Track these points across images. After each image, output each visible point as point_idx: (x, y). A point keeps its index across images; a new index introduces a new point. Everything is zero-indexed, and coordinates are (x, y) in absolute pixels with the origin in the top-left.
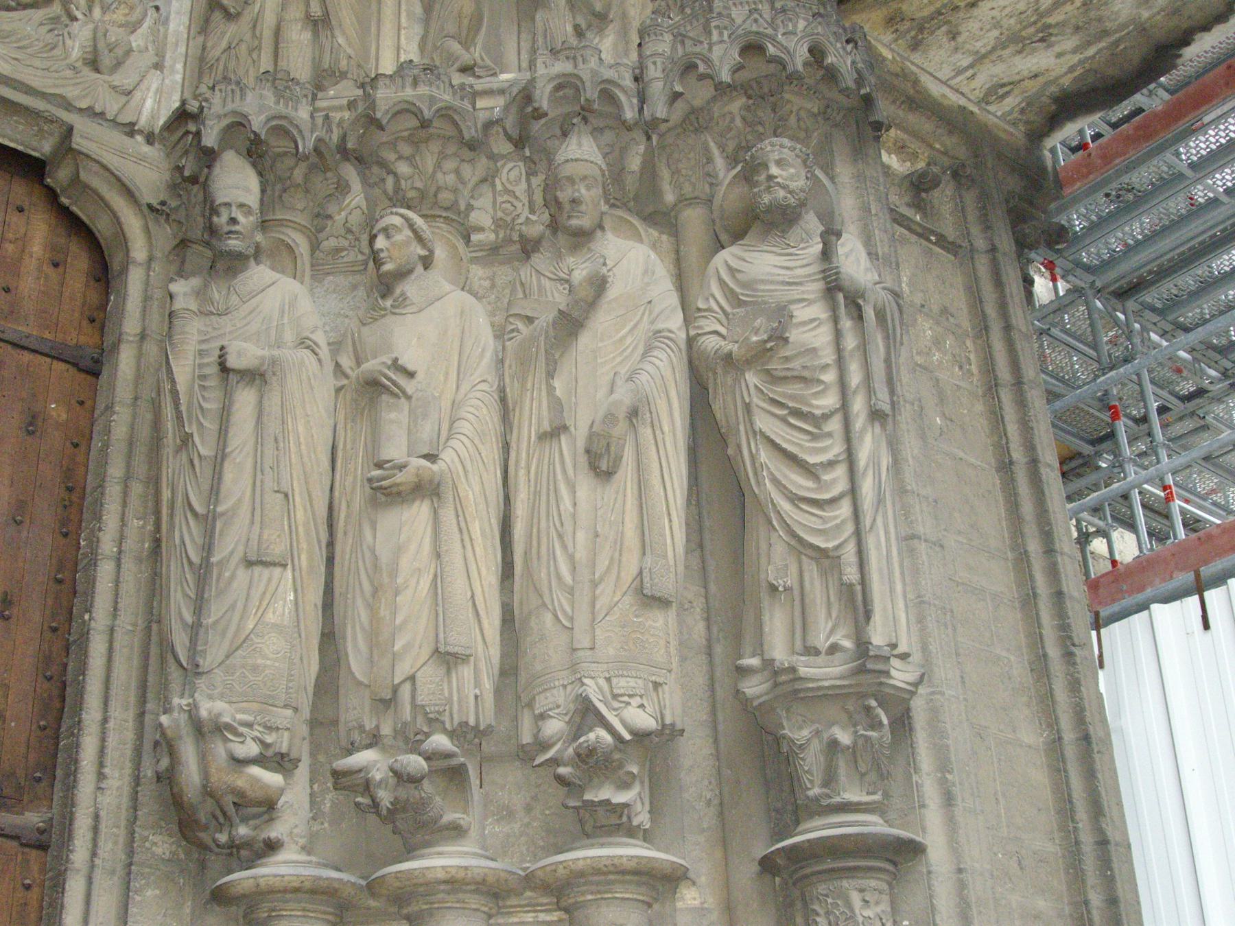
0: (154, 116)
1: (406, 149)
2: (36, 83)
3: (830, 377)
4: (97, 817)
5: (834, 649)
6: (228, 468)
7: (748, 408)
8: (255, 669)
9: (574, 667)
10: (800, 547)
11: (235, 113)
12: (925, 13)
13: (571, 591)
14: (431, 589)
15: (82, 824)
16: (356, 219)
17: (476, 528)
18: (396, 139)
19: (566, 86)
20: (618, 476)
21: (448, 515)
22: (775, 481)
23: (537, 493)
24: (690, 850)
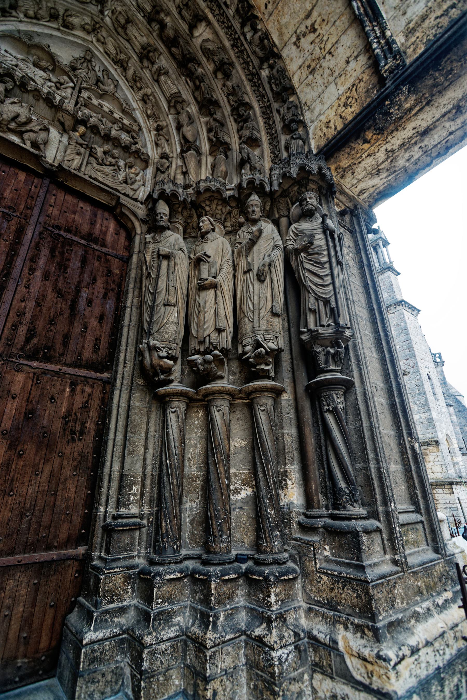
1: (208, 203)
2: (110, 184)
3: (325, 253)
4: (123, 374)
5: (329, 325)
6: (160, 280)
7: (302, 262)
8: (166, 333)
9: (254, 332)
10: (318, 298)
14: (214, 312)
15: (119, 375)
16: (195, 225)
17: (227, 296)
19: (251, 182)
22: (311, 281)
23: (243, 287)
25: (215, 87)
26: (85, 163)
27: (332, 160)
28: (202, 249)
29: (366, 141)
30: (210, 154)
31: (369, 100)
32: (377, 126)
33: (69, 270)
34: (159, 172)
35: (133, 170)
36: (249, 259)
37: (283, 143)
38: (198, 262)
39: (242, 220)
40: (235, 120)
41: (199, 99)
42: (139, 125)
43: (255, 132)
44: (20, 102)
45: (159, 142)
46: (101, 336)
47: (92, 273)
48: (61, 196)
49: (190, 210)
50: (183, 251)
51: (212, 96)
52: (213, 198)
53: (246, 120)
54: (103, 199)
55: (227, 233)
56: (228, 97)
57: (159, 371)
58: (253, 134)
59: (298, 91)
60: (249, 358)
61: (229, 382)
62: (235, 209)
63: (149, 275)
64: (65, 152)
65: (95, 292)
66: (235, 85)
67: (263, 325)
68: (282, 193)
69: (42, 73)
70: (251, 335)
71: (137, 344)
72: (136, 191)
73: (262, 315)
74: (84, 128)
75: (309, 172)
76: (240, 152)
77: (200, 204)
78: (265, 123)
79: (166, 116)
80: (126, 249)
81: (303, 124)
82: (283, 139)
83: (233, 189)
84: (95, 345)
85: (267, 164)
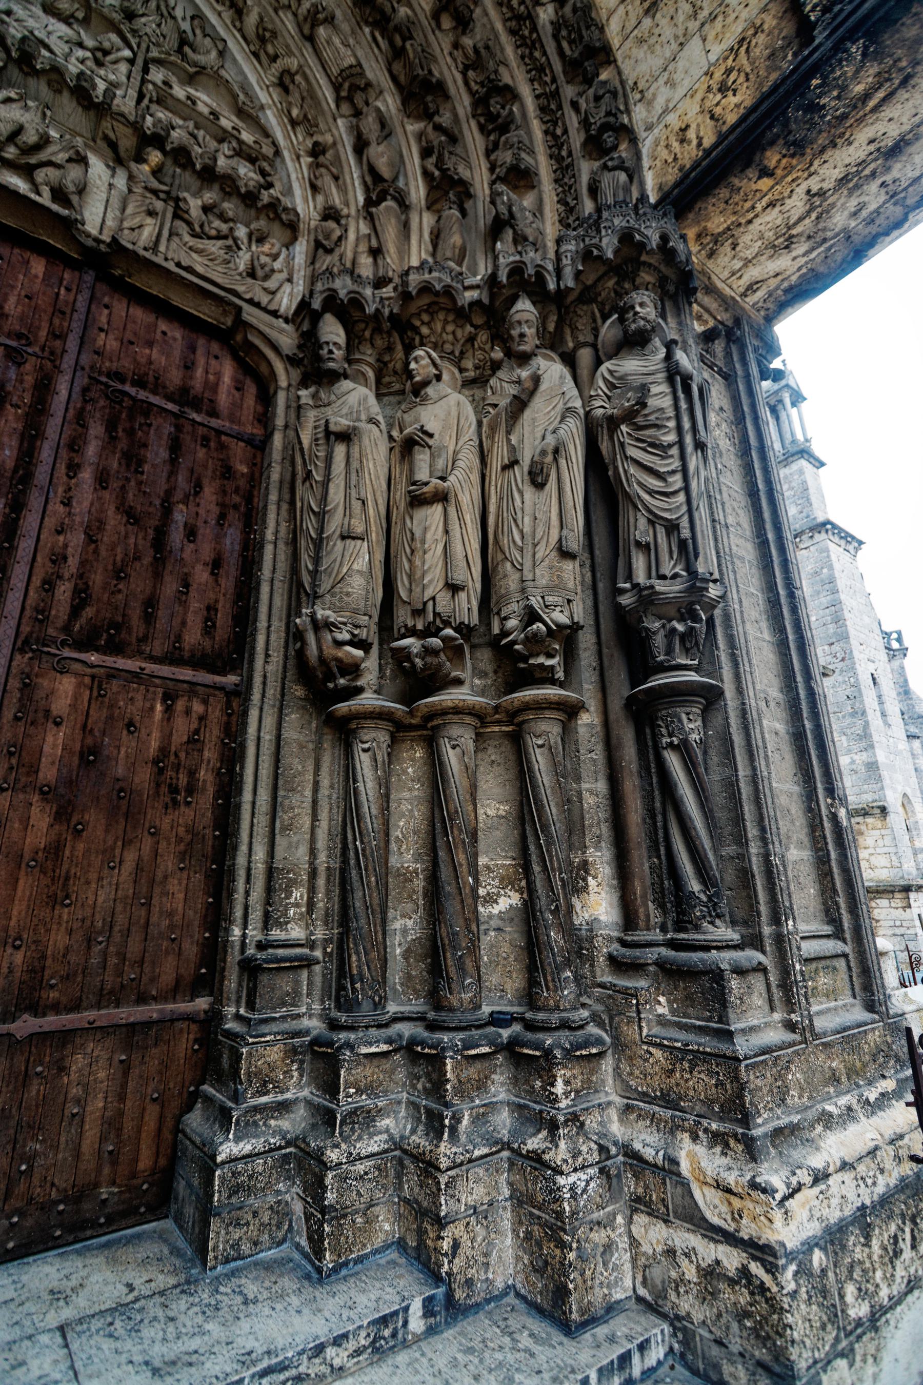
0: (288, 308)
1: (425, 317)
2: (219, 280)
3: (672, 424)
4: (265, 677)
5: (675, 576)
6: (332, 486)
7: (622, 445)
8: (348, 594)
9: (523, 590)
11: (329, 289)
12: (721, 229)
13: (521, 550)
14: (444, 548)
15: (257, 680)
16: (399, 366)
19: (517, 270)
20: (548, 487)
21: (452, 511)
22: (640, 484)
23: (501, 498)
24: (587, 691)
25: (438, 50)
26: (166, 233)
27: (691, 216)
28: (417, 420)
29: (766, 173)
30: (428, 208)
31: (774, 76)
32: (791, 138)
33: (146, 468)
34: (320, 251)
35: (266, 248)
36: (514, 439)
37: (585, 179)
38: (408, 447)
39: (498, 354)
40: (482, 128)
41: (402, 78)
42: (274, 144)
43: (523, 155)
44: (22, 98)
45: (319, 183)
46: (217, 601)
47: (192, 471)
48: (120, 307)
49: (388, 333)
50: (377, 423)
51: (430, 72)
52: (436, 308)
53: (504, 129)
54: (205, 312)
55: (468, 384)
56: (464, 74)
57: (335, 670)
58: (519, 159)
59: (619, 56)
60: (514, 642)
61: (475, 692)
62: (484, 330)
63: (308, 475)
64: (123, 210)
65: (202, 512)
66: (480, 45)
67: (543, 576)
68: (582, 293)
69: (62, 29)
70: (517, 596)
71: (289, 616)
72: (274, 293)
73: (539, 556)
74: (159, 154)
75: (642, 246)
76: (493, 202)
77: (409, 322)
78: (546, 132)
79: (330, 120)
80: (259, 421)
81: (628, 133)
82: (586, 169)
83: (477, 287)
84: (207, 619)
85: (551, 229)
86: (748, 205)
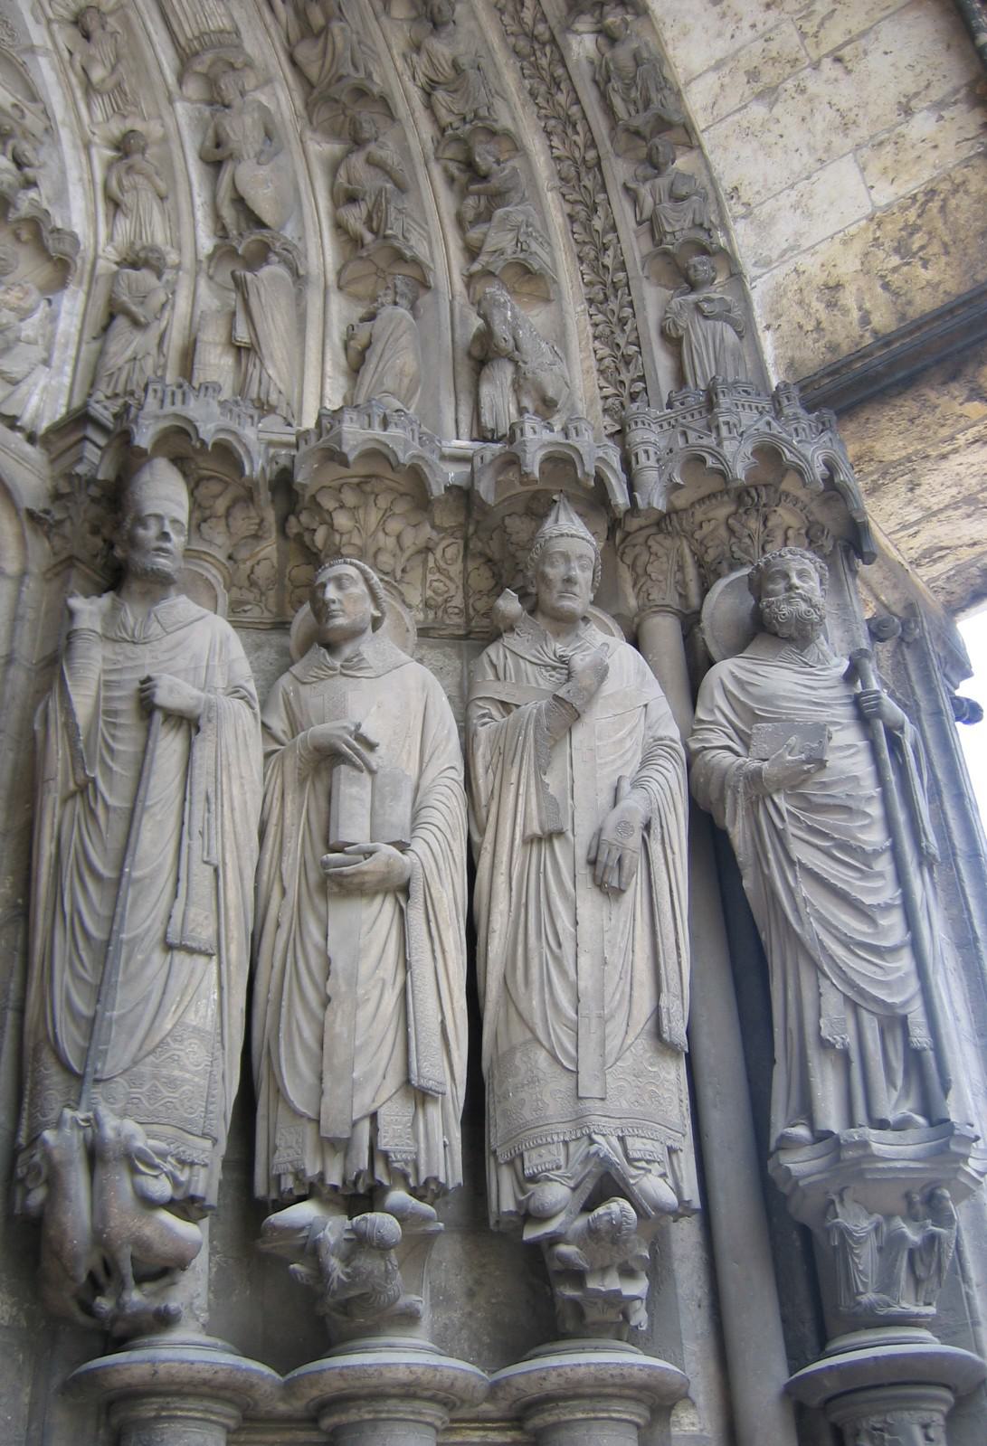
0: (38, 416)
1: (350, 498)
3: (875, 810)
7: (780, 836)
9: (579, 1119)
11: (176, 416)
12: (895, 457)
18: (342, 485)
20: (628, 896)
21: (416, 916)
25: (381, 46)
28: (339, 710)
41: (313, 72)
42: (46, 112)
43: (535, 247)
45: (128, 199)
51: (369, 76)
59: (706, 140)
60: (555, 1239)
61: (443, 1343)
66: (464, 61)
72: (15, 383)
73: (613, 1044)
78: (571, 218)
79: (163, 102)
82: (652, 299)
85: (579, 377)
86: (945, 432)
